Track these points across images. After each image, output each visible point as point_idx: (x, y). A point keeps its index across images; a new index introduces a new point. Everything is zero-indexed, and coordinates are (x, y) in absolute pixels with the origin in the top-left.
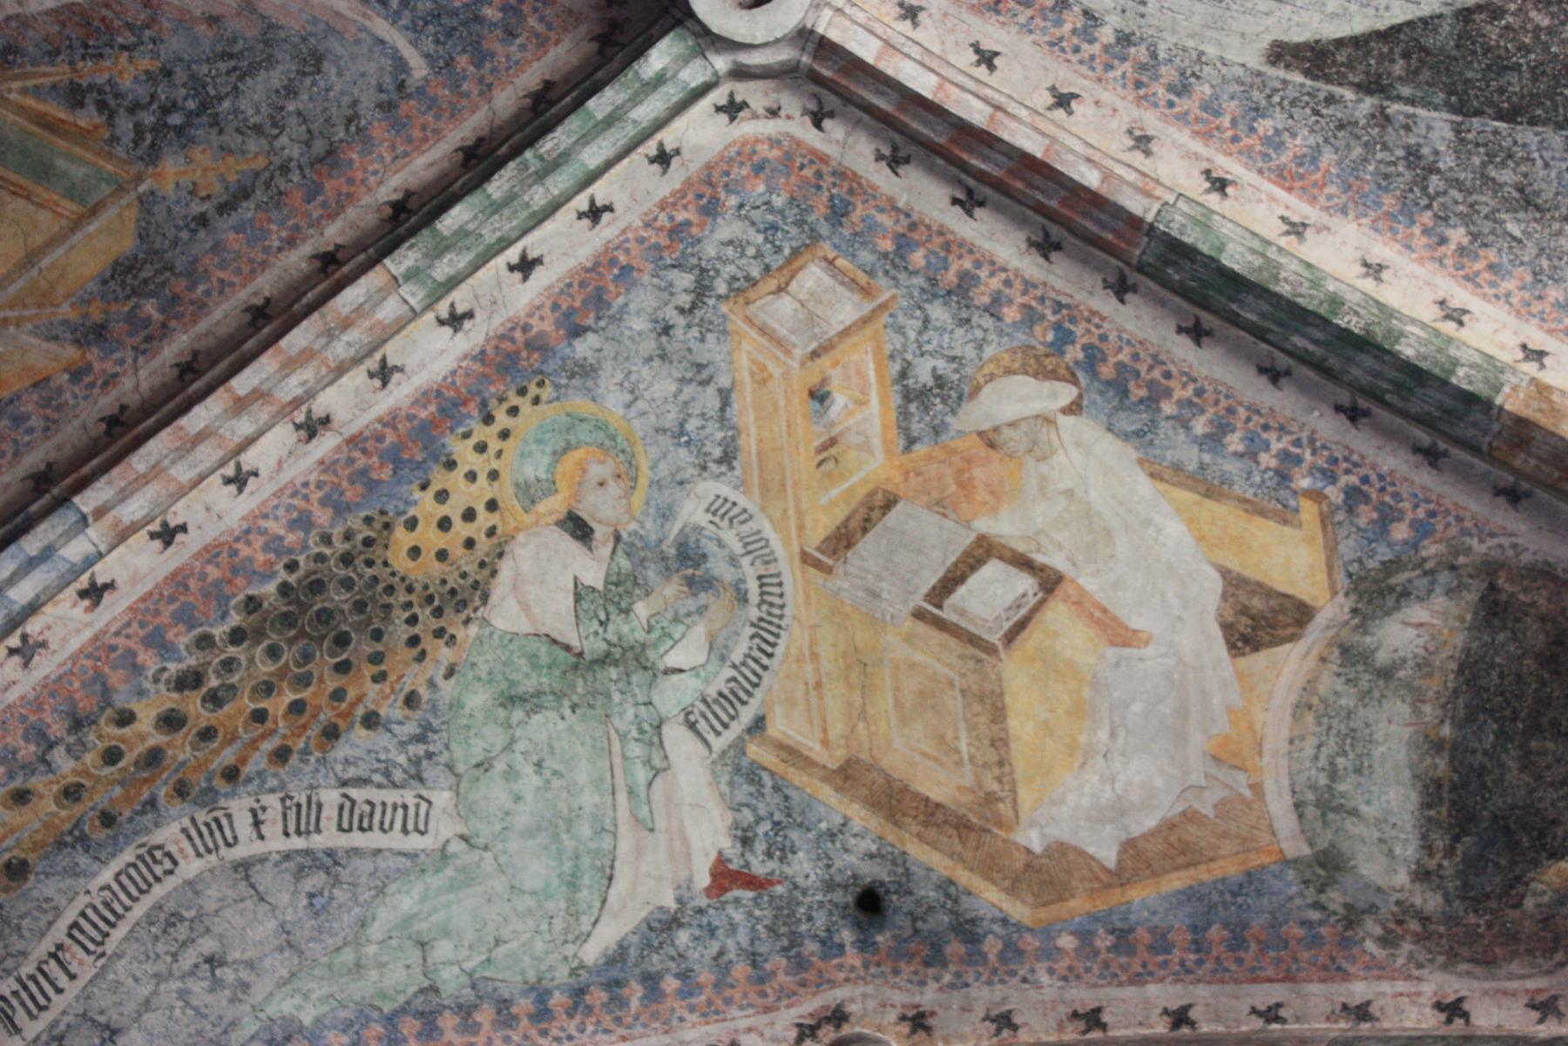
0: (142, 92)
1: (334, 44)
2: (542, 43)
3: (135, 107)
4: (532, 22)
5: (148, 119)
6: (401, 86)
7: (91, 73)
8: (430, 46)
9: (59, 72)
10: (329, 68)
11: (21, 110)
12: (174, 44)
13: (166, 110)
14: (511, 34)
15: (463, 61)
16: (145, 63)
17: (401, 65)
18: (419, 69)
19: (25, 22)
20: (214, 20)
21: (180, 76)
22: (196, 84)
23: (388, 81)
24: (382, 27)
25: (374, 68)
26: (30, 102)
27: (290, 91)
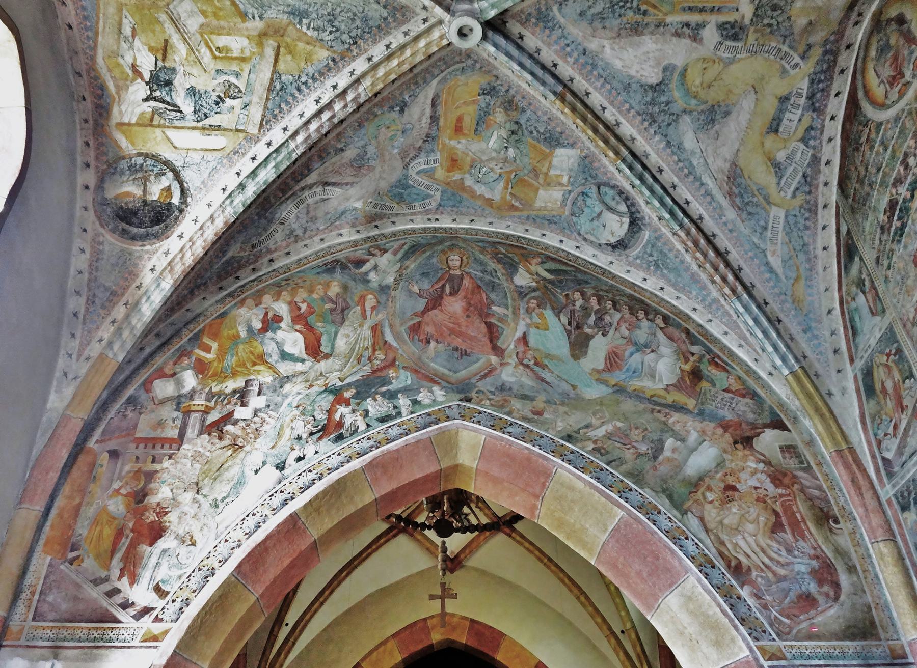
0: (628, 11)
1: (576, 17)
2: (522, 11)
3: (630, 8)
4: (523, 17)
5: (628, 5)
6: (561, 5)
7: (639, 18)
8: (551, 14)
9: (648, 19)
10: (578, 12)
11: (660, 10)
12: (616, 23)
13: (623, 6)
14: (530, 14)
15: (543, 9)
16: (625, 20)
17: (560, 10)
18: (555, 8)
19: (652, 33)
20: (604, 28)
21: (617, 15)
22: (613, 12)
23: (564, 6)
24: (562, 20)
25: (567, 10)
26: (657, 12)
27: (590, 7)
